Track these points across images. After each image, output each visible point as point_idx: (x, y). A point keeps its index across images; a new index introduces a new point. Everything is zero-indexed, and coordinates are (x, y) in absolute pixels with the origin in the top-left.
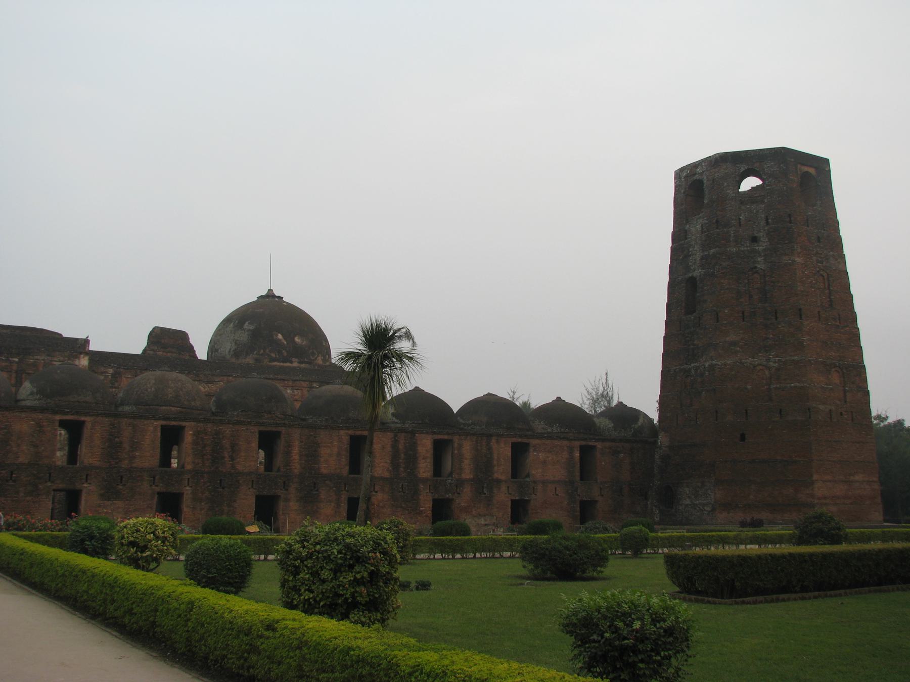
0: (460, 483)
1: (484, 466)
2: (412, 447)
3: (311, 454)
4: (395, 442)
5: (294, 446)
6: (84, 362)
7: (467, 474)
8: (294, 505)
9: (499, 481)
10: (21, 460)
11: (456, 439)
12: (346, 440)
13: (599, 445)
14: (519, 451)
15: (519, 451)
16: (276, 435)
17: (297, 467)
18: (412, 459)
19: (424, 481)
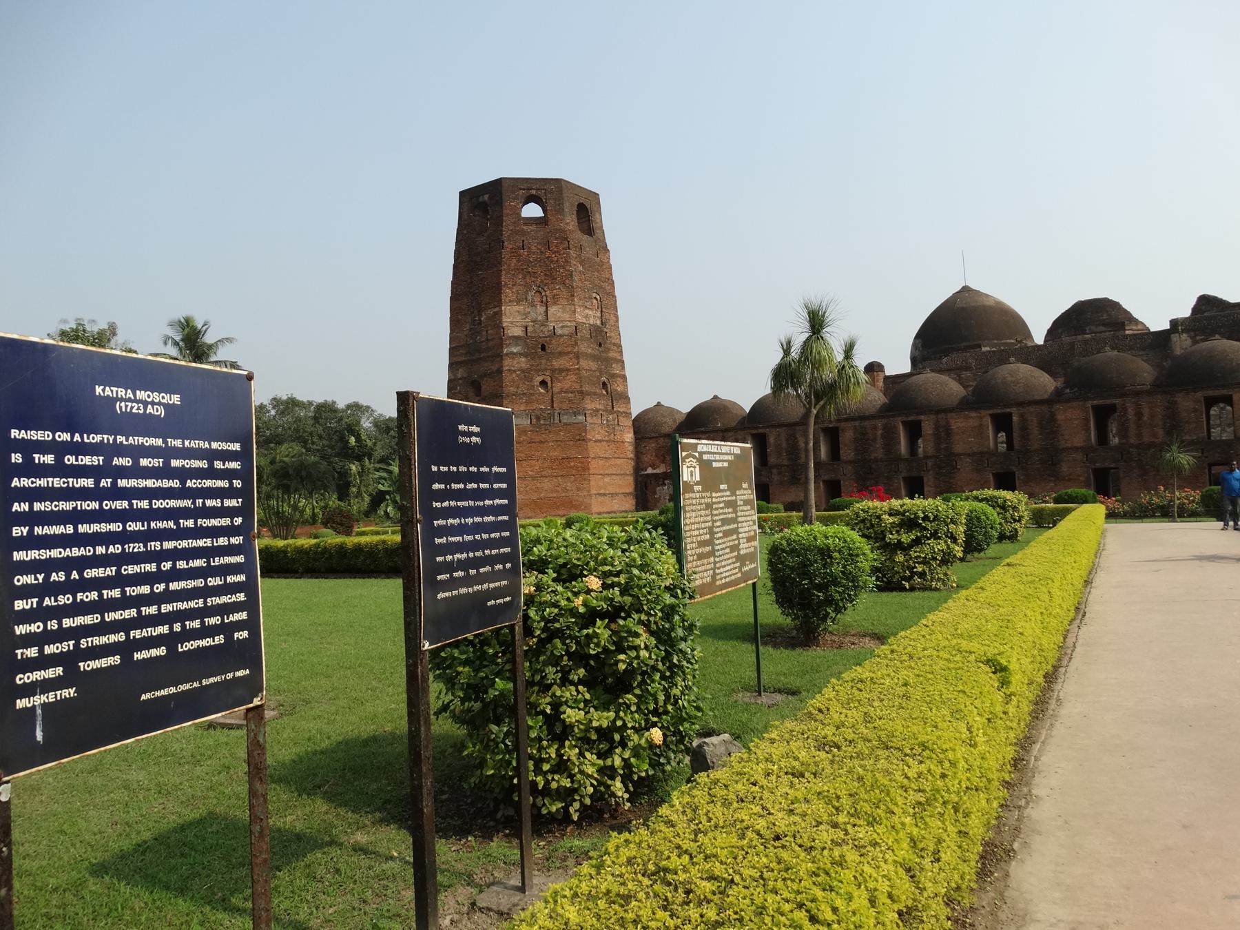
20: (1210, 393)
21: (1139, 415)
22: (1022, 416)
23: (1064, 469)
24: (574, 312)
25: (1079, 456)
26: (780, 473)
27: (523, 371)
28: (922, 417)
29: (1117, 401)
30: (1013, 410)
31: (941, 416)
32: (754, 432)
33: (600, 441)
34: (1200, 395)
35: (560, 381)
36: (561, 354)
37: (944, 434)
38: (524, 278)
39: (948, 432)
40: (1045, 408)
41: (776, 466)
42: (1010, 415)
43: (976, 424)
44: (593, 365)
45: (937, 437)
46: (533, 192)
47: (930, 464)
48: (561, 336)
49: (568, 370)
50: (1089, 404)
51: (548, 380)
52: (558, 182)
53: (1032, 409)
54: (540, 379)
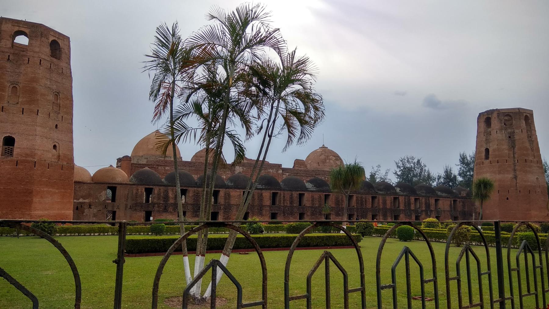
0: (422, 211)
1: (428, 205)
2: (409, 200)
3: (385, 203)
4: (405, 199)
5: (380, 199)
6: (281, 172)
7: (424, 209)
8: (381, 217)
9: (432, 211)
10: (317, 205)
11: (420, 198)
12: (393, 198)
13: (458, 200)
14: (436, 201)
15: (436, 201)
16: (376, 197)
17: (381, 207)
18: (409, 204)
19: (413, 210)
20: (300, 192)
21: (284, 197)
23: (264, 212)
25: (268, 208)
26: (158, 207)
28: (221, 189)
29: (279, 192)
31: (227, 190)
34: (298, 193)
37: (228, 197)
40: (260, 191)
41: (157, 203)
43: (239, 194)
45: (225, 199)
47: (222, 207)
50: (272, 191)
51: (57, 145)
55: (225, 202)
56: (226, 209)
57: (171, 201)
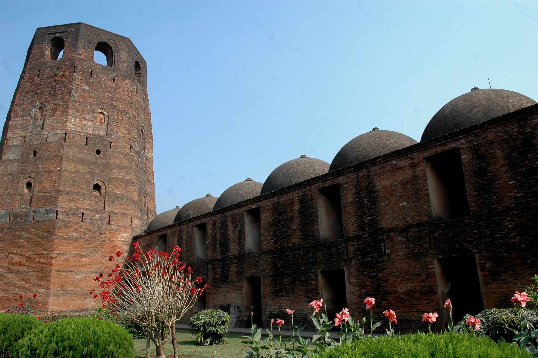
22: (475, 150)
24: (66, 121)
27: (12, 174)
30: (461, 143)
31: (363, 172)
32: (198, 222)
33: (76, 239)
35: (41, 182)
36: (47, 158)
38: (32, 98)
39: (371, 191)
42: (456, 151)
44: (82, 169)
46: (58, 35)
47: (352, 249)
48: (51, 143)
49: (50, 171)
52: (77, 25)
53: (490, 135)
54: (26, 181)
55: (362, 227)
56: (365, 255)
57: (234, 249)
